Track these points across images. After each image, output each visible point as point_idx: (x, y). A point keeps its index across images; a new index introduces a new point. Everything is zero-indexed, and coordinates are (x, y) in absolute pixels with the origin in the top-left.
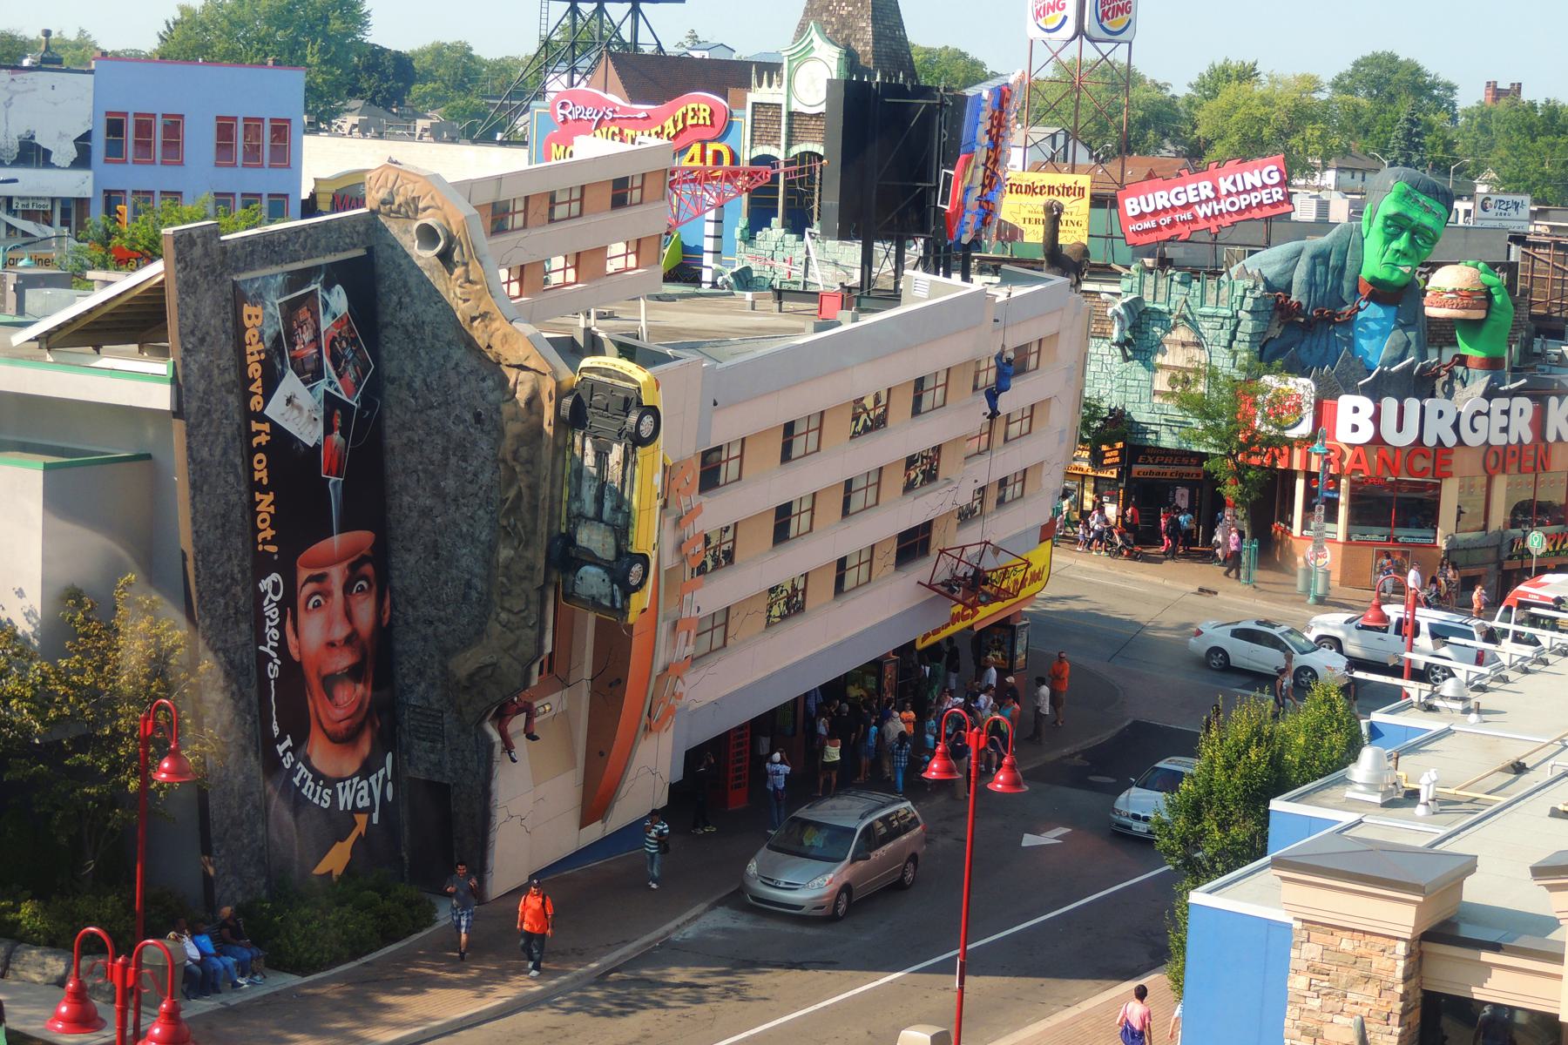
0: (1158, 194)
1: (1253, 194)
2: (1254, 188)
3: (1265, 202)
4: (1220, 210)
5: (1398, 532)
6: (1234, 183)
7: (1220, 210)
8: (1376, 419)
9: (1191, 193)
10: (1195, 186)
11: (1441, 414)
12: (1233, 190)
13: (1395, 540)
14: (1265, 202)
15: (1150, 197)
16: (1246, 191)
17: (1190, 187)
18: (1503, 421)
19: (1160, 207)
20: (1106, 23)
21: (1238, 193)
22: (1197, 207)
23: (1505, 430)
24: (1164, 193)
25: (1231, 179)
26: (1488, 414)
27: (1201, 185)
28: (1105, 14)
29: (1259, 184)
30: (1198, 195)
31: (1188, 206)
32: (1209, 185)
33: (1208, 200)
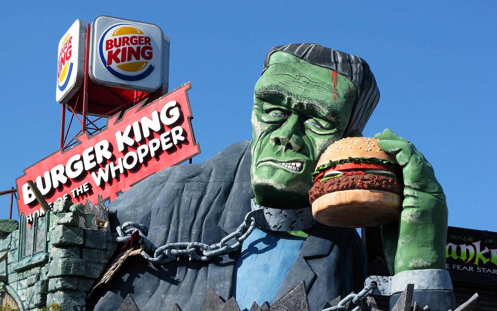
0: (53, 171)
1: (151, 143)
3: (165, 147)
4: (117, 171)
6: (131, 135)
7: (117, 171)
9: (87, 158)
10: (91, 149)
12: (131, 142)
15: (47, 176)
16: (143, 141)
19: (56, 185)
20: (114, 65)
21: (135, 146)
24: (60, 167)
29: (157, 128)
30: (95, 160)
32: (105, 144)
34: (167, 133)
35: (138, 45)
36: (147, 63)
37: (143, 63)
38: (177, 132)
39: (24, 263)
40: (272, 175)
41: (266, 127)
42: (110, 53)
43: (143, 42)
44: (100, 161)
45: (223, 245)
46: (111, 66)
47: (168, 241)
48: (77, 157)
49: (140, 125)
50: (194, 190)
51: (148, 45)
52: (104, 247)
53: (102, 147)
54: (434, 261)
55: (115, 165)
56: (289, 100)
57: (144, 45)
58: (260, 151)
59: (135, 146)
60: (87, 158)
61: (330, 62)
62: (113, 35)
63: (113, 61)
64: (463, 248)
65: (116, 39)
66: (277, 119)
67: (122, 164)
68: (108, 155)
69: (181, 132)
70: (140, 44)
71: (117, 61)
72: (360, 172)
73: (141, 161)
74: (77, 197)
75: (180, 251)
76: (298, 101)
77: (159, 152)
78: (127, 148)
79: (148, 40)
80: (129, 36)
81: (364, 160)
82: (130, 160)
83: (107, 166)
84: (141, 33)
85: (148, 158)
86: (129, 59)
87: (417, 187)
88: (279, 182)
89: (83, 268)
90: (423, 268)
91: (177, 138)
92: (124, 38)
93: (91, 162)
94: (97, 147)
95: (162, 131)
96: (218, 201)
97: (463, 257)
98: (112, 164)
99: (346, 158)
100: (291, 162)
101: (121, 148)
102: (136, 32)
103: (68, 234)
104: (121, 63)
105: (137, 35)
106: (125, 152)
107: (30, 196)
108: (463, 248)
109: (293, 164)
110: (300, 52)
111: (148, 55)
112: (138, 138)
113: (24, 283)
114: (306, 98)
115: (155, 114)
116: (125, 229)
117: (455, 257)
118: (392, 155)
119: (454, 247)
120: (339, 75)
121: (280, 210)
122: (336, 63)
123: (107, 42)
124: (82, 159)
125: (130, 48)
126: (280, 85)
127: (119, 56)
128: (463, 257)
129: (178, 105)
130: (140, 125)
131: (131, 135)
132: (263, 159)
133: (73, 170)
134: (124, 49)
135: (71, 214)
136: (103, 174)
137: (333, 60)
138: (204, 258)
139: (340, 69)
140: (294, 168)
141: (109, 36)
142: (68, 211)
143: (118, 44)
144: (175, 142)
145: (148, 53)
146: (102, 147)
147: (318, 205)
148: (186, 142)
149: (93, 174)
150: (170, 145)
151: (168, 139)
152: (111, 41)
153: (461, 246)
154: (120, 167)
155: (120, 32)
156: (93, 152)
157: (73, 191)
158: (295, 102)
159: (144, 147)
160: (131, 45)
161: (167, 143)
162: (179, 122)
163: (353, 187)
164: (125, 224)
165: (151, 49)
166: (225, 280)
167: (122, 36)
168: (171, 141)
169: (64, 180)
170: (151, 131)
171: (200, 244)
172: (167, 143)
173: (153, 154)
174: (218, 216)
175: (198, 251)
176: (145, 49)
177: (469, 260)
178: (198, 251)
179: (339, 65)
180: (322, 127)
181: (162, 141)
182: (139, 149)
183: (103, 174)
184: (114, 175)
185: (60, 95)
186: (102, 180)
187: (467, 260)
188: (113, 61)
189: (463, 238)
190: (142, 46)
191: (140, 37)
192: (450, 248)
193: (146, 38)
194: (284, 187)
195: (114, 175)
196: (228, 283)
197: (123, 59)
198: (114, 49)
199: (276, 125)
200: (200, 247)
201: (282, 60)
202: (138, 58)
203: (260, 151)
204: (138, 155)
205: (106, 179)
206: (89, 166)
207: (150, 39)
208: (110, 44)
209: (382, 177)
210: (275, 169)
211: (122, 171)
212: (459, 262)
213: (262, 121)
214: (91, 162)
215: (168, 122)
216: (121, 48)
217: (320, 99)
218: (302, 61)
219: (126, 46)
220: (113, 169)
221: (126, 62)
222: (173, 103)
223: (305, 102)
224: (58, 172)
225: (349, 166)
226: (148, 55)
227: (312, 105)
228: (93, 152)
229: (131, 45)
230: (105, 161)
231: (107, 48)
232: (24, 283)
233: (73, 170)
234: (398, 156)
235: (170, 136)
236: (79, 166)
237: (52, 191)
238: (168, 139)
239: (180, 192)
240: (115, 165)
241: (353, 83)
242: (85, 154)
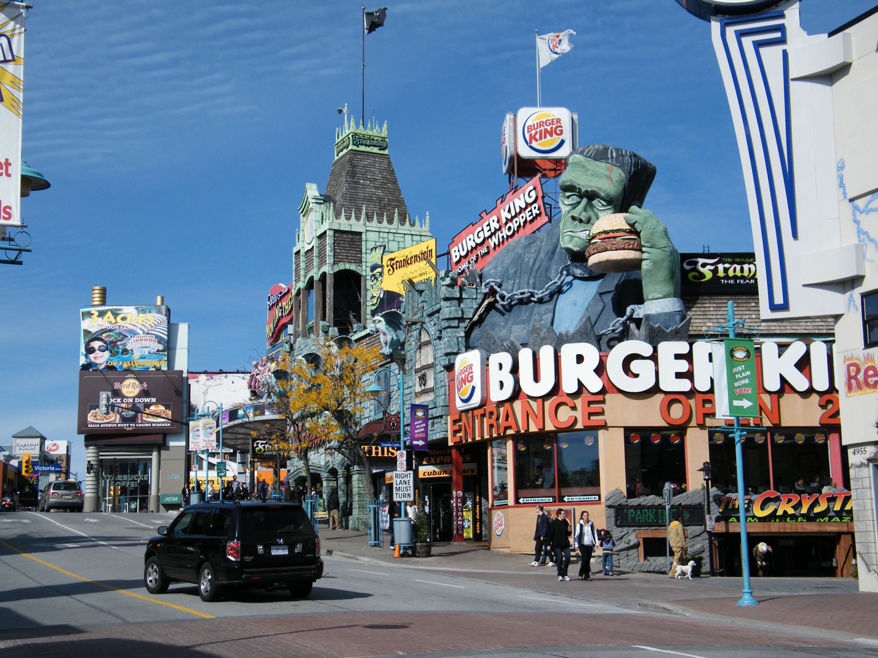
0: (468, 239)
3: (529, 219)
4: (503, 237)
6: (509, 211)
8: (515, 370)
9: (486, 229)
10: (487, 223)
11: (580, 359)
12: (509, 217)
15: (464, 242)
16: (516, 215)
19: (469, 249)
20: (534, 144)
21: (513, 218)
24: (471, 236)
26: (654, 358)
28: (532, 137)
29: (523, 206)
30: (490, 230)
32: (495, 218)
34: (529, 209)
35: (551, 126)
36: (559, 138)
37: (556, 138)
38: (535, 208)
39: (430, 310)
40: (571, 241)
41: (568, 208)
42: (531, 135)
43: (555, 123)
44: (493, 230)
45: (547, 290)
46: (532, 145)
47: (515, 289)
48: (480, 229)
49: (514, 203)
50: (532, 253)
51: (559, 124)
52: (475, 297)
53: (493, 221)
54: (665, 293)
55: (502, 233)
56: (580, 189)
57: (556, 125)
58: (565, 224)
59: (513, 218)
60: (486, 229)
61: (607, 158)
62: (532, 121)
63: (533, 141)
64: (746, 267)
65: (534, 124)
66: (574, 202)
67: (505, 232)
68: (497, 227)
69: (537, 208)
70: (553, 124)
71: (536, 140)
72: (612, 239)
73: (516, 229)
74: (482, 256)
75: (520, 296)
76: (585, 189)
77: (525, 222)
78: (508, 221)
79: (558, 121)
80: (544, 120)
81: (613, 231)
83: (497, 234)
84: (554, 116)
85: (519, 227)
86: (545, 137)
87: (649, 246)
88: (575, 246)
89: (460, 312)
90: (658, 299)
91: (536, 212)
92: (540, 122)
93: (488, 231)
95: (526, 208)
96: (548, 258)
97: (746, 274)
98: (500, 232)
99: (602, 231)
100: (582, 231)
101: (504, 221)
102: (550, 116)
103: (449, 291)
104: (539, 142)
105: (550, 119)
106: (506, 223)
107: (456, 256)
108: (746, 267)
109: (584, 232)
110: (587, 153)
111: (559, 132)
112: (513, 214)
113: (432, 323)
114: (589, 187)
115: (522, 195)
116: (488, 284)
117: (739, 274)
118: (632, 225)
119: (738, 267)
120: (614, 167)
121: (581, 264)
122: (612, 157)
123: (528, 127)
124: (483, 230)
125: (546, 130)
126: (573, 179)
127: (538, 136)
128: (746, 274)
129: (535, 189)
130: (514, 203)
131: (509, 211)
132: (565, 231)
133: (479, 237)
134: (541, 131)
135: (449, 279)
136: (495, 240)
137: (609, 156)
138: (535, 299)
139: (614, 162)
140: (585, 235)
141: (529, 123)
142: (448, 277)
143: (536, 127)
144: (534, 215)
145: (559, 131)
146: (493, 221)
147: (593, 260)
148: (540, 213)
149: (490, 239)
150: (531, 217)
151: (530, 213)
152: (531, 126)
153: (743, 266)
155: (537, 118)
156: (489, 225)
157: (479, 252)
158: (583, 190)
159: (517, 219)
160: (546, 127)
161: (530, 216)
162: (535, 201)
163: (606, 250)
164: (487, 281)
165: (561, 127)
166: (548, 313)
167: (538, 121)
168: (532, 214)
169: (474, 245)
170: (520, 207)
171: (533, 291)
172: (530, 216)
173: (522, 224)
174: (547, 270)
175: (532, 295)
176: (556, 128)
177: (751, 275)
178: (532, 295)
179: (614, 159)
180: (603, 205)
181: (526, 215)
182: (514, 220)
183: (495, 240)
184: (501, 240)
185: (504, 169)
186: (495, 243)
187: (749, 275)
188: (533, 141)
189: (745, 259)
190: (554, 126)
191: (552, 120)
192: (735, 269)
193: (557, 119)
194: (578, 249)
195: (501, 240)
196: (551, 315)
197: (541, 139)
198: (533, 132)
199: (575, 206)
200: (534, 292)
201: (576, 161)
202: (551, 136)
203: (565, 224)
204: (514, 225)
205: (497, 243)
206: (487, 234)
207: (560, 120)
208: (530, 128)
209: (627, 241)
210: (573, 237)
211: (505, 237)
212: (743, 277)
213: (565, 204)
214: (488, 231)
215: (530, 201)
216: (538, 130)
217: (599, 186)
218: (589, 159)
219: (542, 128)
220: (501, 236)
221: (543, 140)
222: (531, 188)
223: (589, 190)
224: (470, 239)
226: (559, 132)
227: (594, 191)
228: (489, 225)
229: (546, 127)
230: (496, 230)
231: (528, 132)
232: (432, 323)
233: (479, 237)
234: (635, 225)
235: (531, 211)
236: (481, 234)
237: (468, 251)
238: (530, 213)
239: (522, 255)
240: (502, 233)
241: (623, 171)
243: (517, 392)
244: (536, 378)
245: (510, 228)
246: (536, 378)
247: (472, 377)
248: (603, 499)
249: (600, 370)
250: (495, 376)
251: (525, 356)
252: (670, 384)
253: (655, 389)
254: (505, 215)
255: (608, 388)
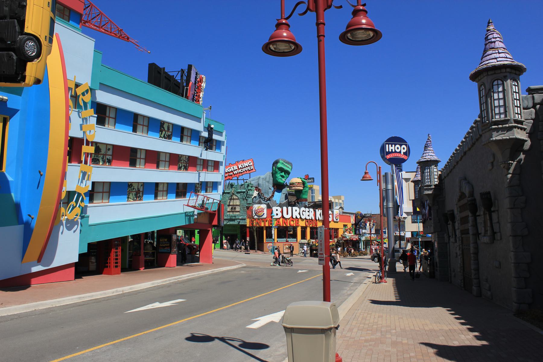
1: (246, 168)
2: (247, 167)
3: (249, 169)
5: (288, 240)
6: (242, 166)
7: (239, 172)
8: (282, 212)
9: (232, 169)
10: (233, 167)
11: (296, 210)
12: (242, 167)
13: (288, 241)
14: (249, 169)
16: (245, 167)
17: (232, 167)
18: (308, 214)
21: (243, 168)
22: (234, 172)
23: (309, 216)
25: (241, 165)
26: (305, 211)
27: (234, 167)
29: (248, 166)
30: (234, 169)
31: (232, 171)
33: (236, 170)
59: (243, 168)
60: (232, 169)
67: (240, 171)
82: (242, 170)
94: (234, 167)
101: (240, 168)
112: (243, 167)
154: (240, 171)
182: (244, 169)
205: (237, 173)
222: (251, 162)
225: (298, 183)
236: (230, 170)
242: (232, 167)
243: (283, 217)
244: (287, 214)
245: (242, 170)
246: (287, 214)
247: (264, 211)
248: (298, 242)
249: (299, 214)
250: (275, 213)
251: (285, 208)
252: (308, 218)
253: (306, 219)
254: (240, 166)
255: (301, 218)
